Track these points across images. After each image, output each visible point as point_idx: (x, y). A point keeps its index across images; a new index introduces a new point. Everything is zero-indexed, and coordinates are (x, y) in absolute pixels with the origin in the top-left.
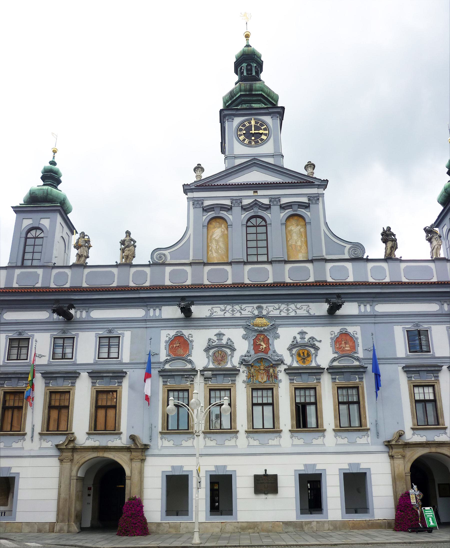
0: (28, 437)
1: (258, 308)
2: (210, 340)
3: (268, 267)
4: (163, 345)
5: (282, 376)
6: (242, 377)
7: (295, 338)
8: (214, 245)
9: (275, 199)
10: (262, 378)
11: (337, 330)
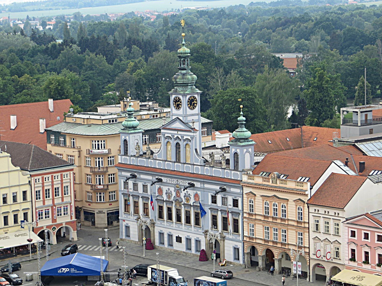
0: (131, 215)
1: (177, 181)
2: (166, 190)
3: (180, 164)
4: (157, 190)
5: (182, 206)
6: (174, 204)
7: (185, 193)
8: (168, 152)
9: (183, 137)
10: (178, 206)
11: (195, 192)
